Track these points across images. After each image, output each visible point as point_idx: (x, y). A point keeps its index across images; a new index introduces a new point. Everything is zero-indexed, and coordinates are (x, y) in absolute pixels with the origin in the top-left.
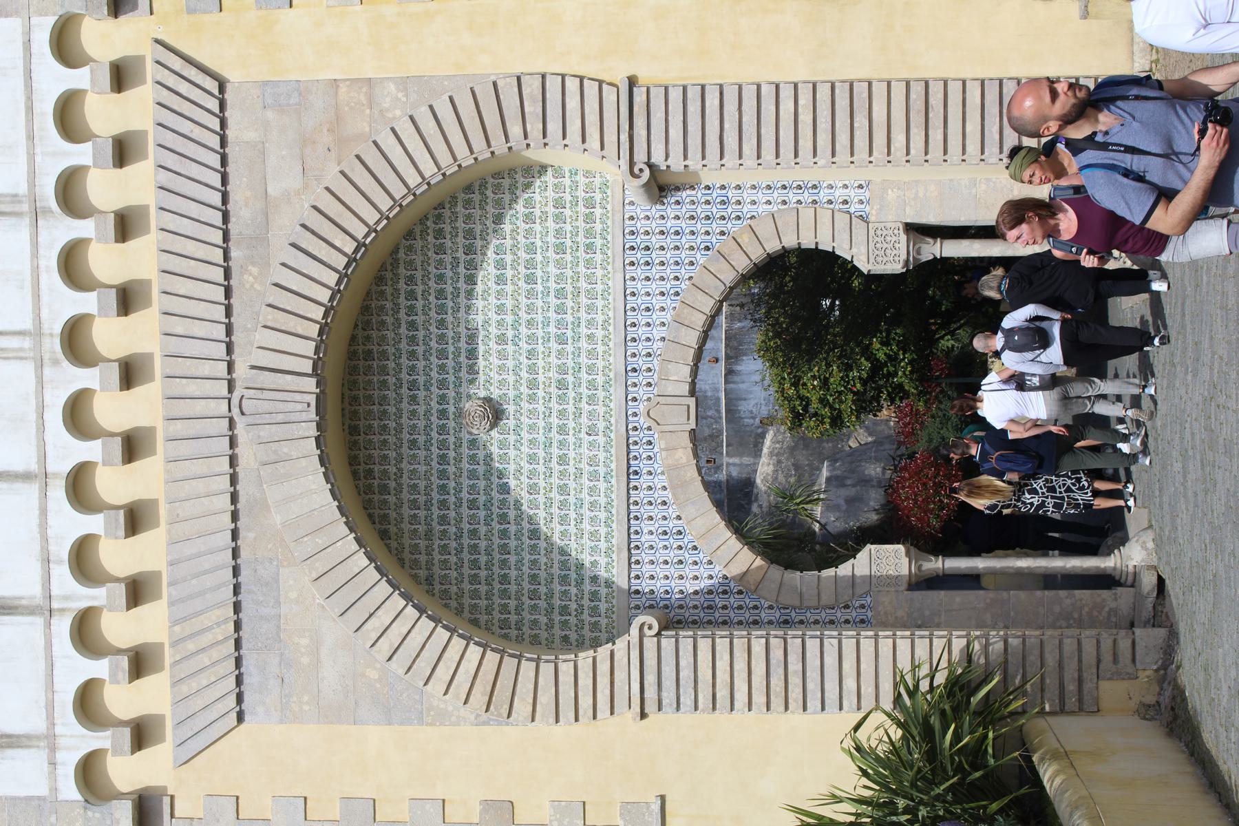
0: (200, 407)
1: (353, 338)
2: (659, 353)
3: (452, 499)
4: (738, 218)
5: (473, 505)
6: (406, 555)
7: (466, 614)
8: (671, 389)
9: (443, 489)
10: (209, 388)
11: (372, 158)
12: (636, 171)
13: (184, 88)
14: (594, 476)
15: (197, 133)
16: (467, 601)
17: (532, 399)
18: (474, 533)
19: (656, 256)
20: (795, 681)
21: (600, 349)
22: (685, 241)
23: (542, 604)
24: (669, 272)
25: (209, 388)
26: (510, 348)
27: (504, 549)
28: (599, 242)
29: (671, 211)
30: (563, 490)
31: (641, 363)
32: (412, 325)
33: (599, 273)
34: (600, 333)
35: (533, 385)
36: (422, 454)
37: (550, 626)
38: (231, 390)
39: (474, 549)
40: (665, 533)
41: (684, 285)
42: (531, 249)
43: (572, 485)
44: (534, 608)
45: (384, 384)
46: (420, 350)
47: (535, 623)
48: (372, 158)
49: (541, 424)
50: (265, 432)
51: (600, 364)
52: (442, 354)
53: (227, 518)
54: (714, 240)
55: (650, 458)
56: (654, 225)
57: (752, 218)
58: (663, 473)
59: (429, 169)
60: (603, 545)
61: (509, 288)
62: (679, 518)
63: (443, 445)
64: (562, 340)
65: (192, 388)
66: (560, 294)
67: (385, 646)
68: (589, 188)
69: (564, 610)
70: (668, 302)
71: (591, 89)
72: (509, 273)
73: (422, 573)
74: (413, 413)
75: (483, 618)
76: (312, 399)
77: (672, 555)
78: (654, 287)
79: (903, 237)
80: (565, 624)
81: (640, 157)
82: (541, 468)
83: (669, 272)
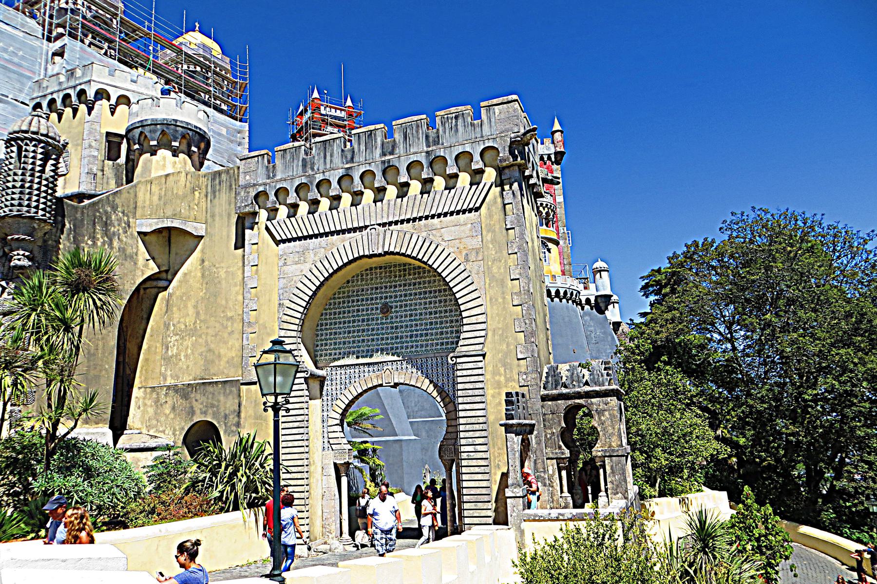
3: (359, 303)
5: (358, 311)
6: (342, 290)
7: (324, 312)
12: (453, 359)
15: (461, 202)
16: (328, 311)
17: (392, 328)
20: (291, 425)
23: (328, 337)
27: (344, 322)
34: (413, 349)
37: (322, 340)
42: (441, 323)
44: (327, 334)
47: (322, 335)
61: (428, 316)
64: (411, 336)
66: (427, 335)
69: (326, 345)
71: (481, 340)
73: (336, 296)
75: (323, 317)
80: (322, 345)
81: (459, 360)
82: (370, 333)
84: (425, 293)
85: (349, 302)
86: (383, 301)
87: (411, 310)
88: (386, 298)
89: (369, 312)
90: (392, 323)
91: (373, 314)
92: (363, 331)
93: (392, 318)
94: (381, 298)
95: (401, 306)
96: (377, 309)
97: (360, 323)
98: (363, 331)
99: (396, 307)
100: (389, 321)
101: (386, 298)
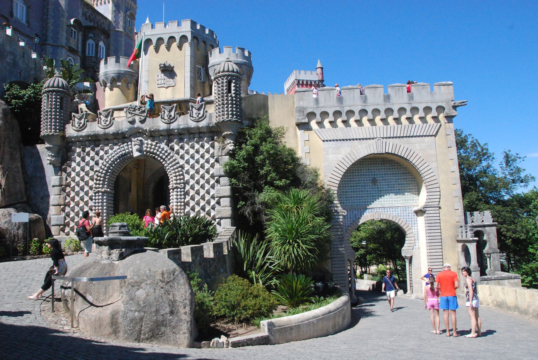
0: (378, 132)
1: (387, 158)
5: (359, 181)
8: (381, 215)
9: (361, 175)
10: (382, 134)
11: (424, 162)
13: (433, 129)
14: (365, 202)
17: (378, 191)
18: (354, 181)
19: (405, 212)
21: (388, 203)
22: (407, 217)
23: (342, 194)
24: (402, 214)
25: (382, 134)
26: (387, 186)
27: (351, 186)
28: (406, 202)
29: (412, 214)
30: (362, 197)
31: (386, 210)
32: (390, 169)
33: (401, 202)
35: (381, 191)
36: (367, 171)
38: (382, 138)
39: (351, 181)
41: (400, 217)
43: (363, 198)
45: (379, 164)
46: (386, 170)
48: (424, 162)
49: (374, 192)
50: (375, 144)
51: (385, 203)
52: (385, 174)
53: (359, 138)
56: (410, 212)
59: (422, 172)
60: (353, 204)
61: (397, 186)
63: (369, 175)
65: (382, 131)
67: (338, 166)
68: (416, 200)
70: (397, 215)
72: (400, 186)
74: (374, 169)
76: (381, 152)
77: (352, 216)
78: (399, 212)
79: (410, 256)
81: (427, 209)
82: (366, 192)
83: (402, 214)
84: (396, 174)
85: (353, 176)
86: (373, 176)
87: (388, 182)
88: (375, 175)
89: (365, 182)
90: (378, 188)
91: (367, 183)
92: (362, 191)
93: (378, 185)
94: (372, 175)
95: (383, 180)
96: (370, 180)
97: (360, 187)
98: (362, 191)
99: (380, 180)
100: (376, 187)
101: (375, 175)
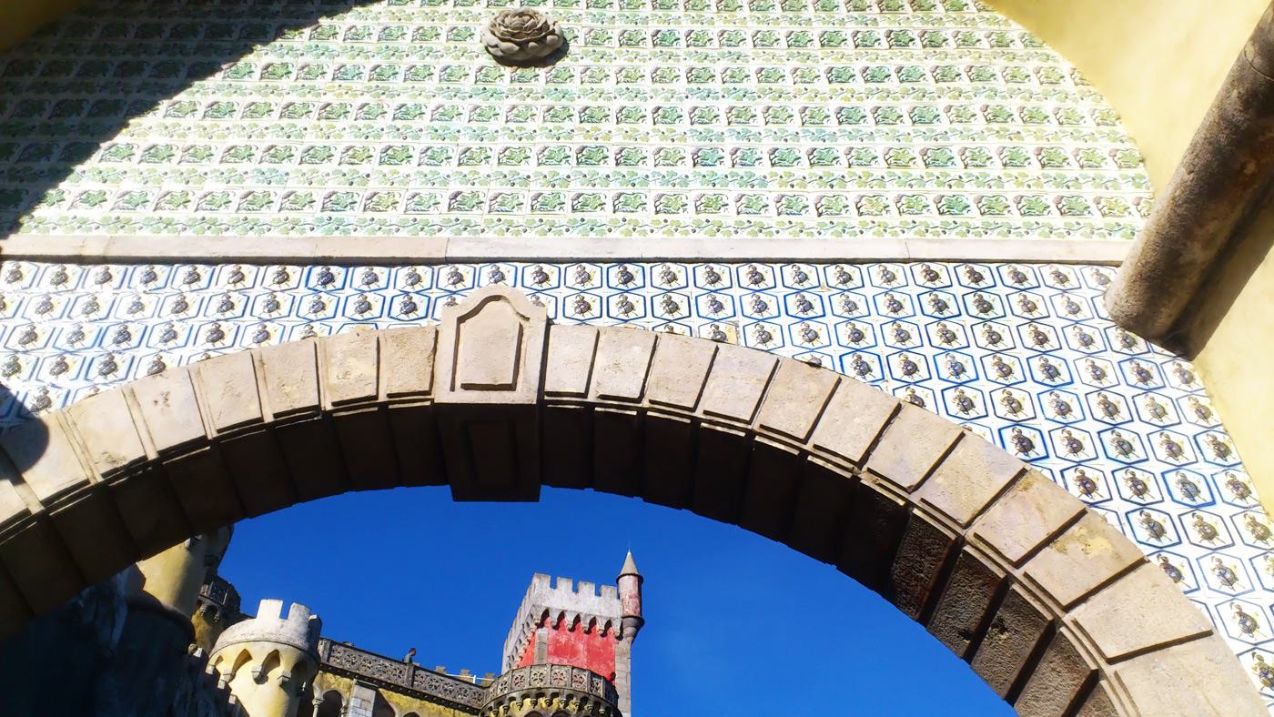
2: (677, 329)
4: (1158, 531)
40: (124, 336)
54: (1055, 464)
55: (365, 307)
57: (1168, 567)
58: (311, 333)
62: (159, 368)
